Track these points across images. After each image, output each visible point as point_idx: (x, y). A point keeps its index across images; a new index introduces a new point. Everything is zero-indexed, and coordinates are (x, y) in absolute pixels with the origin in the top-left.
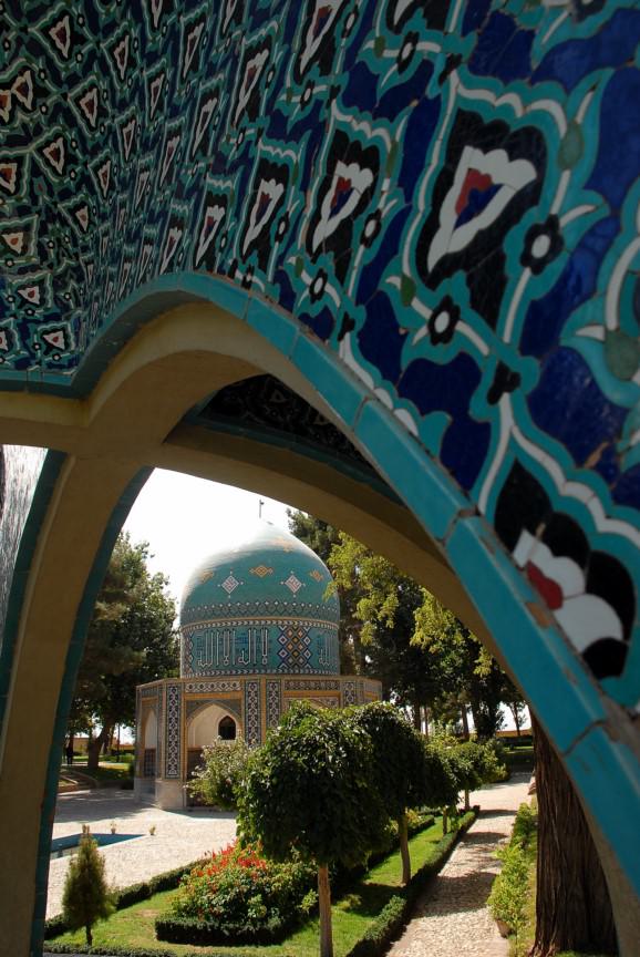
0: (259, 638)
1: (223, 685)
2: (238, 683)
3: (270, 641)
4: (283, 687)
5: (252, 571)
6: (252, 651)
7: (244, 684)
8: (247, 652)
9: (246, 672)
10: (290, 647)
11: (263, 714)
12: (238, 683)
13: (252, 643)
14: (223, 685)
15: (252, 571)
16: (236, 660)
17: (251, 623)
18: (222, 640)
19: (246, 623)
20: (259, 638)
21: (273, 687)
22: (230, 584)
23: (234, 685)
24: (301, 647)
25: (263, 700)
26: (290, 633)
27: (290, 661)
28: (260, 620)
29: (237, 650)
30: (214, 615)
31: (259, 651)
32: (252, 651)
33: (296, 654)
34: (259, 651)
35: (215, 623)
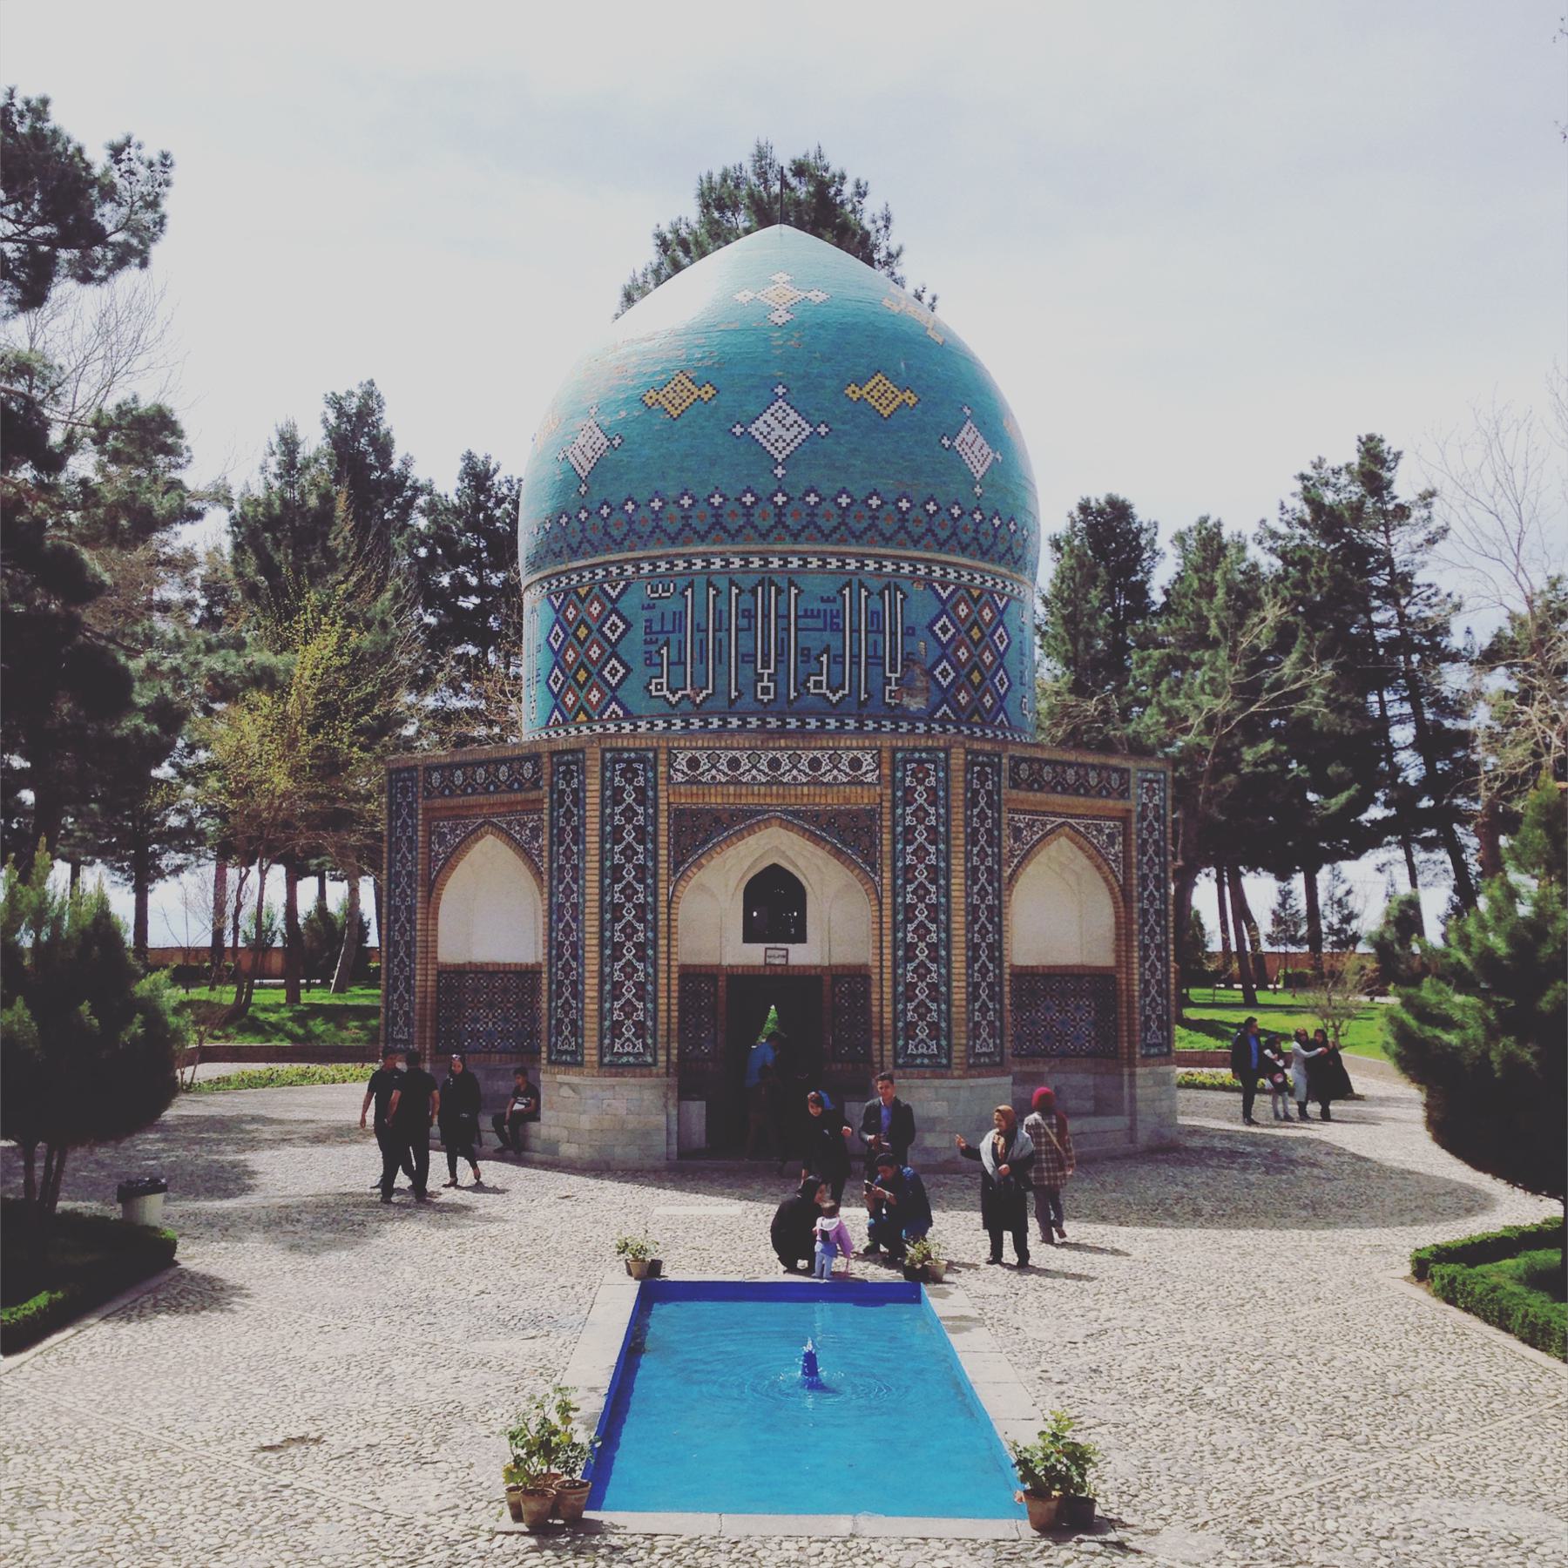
0: (875, 617)
1: (815, 764)
2: (867, 760)
3: (909, 632)
4: (1005, 783)
5: (853, 392)
6: (855, 658)
7: (895, 761)
8: (837, 659)
9: (833, 724)
10: (963, 654)
11: (958, 865)
12: (867, 760)
13: (855, 630)
14: (815, 764)
15: (853, 392)
16: (801, 685)
17: (853, 564)
18: (749, 614)
19: (834, 563)
20: (875, 617)
21: (982, 777)
22: (780, 429)
23: (856, 764)
24: (988, 658)
25: (958, 817)
26: (963, 610)
27: (963, 698)
28: (879, 559)
29: (804, 653)
30: (718, 527)
31: (875, 659)
32: (855, 658)
33: (976, 677)
34: (875, 659)
35: (723, 557)
